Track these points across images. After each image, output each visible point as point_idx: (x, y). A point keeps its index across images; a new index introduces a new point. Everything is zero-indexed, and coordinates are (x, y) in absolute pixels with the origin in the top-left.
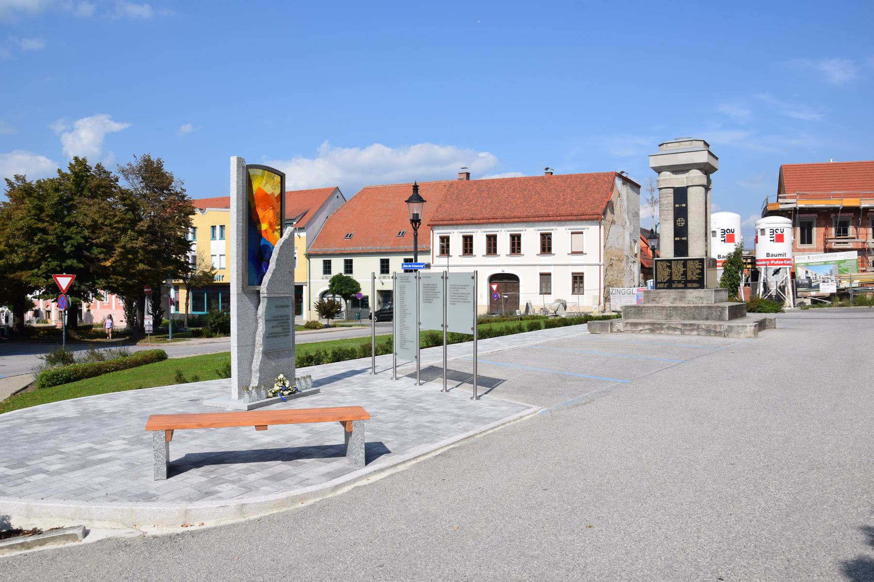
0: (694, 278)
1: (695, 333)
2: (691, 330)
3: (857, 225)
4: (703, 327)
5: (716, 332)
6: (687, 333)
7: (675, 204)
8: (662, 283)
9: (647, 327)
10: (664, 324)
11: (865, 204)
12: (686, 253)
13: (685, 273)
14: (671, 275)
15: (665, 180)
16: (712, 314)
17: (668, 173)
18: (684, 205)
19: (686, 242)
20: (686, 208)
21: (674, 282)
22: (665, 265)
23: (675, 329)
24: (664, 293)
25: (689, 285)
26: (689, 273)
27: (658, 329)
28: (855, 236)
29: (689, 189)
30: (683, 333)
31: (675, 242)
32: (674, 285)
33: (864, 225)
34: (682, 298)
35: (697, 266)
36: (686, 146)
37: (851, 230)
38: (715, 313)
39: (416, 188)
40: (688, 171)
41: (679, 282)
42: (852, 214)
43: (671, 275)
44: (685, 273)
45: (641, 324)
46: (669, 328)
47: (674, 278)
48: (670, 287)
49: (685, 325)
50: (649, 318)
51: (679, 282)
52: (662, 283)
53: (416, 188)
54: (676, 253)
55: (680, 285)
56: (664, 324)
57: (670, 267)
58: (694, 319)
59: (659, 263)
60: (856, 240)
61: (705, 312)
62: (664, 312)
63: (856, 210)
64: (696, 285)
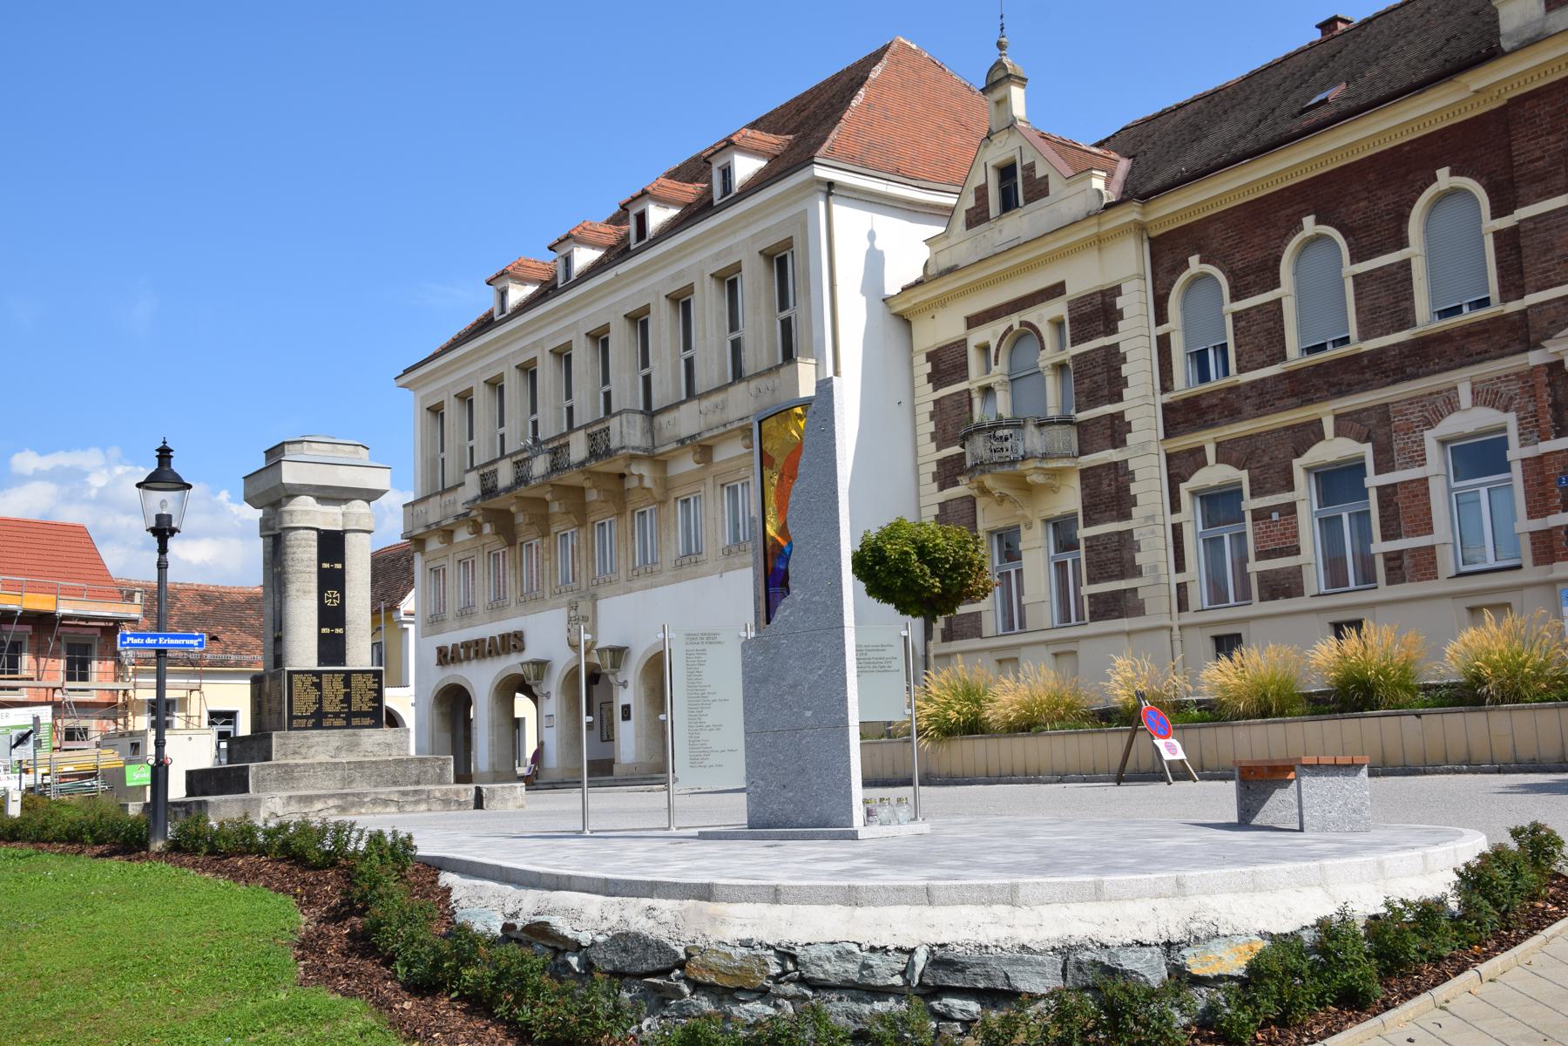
0: (365, 708)
1: (423, 807)
2: (417, 802)
3: (39, 652)
4: (438, 794)
5: (460, 804)
6: (408, 808)
7: (320, 562)
8: (302, 717)
9: (331, 803)
10: (366, 795)
11: (64, 609)
12: (341, 659)
13: (347, 699)
14: (320, 701)
15: (307, 512)
16: (426, 772)
17: (311, 500)
18: (338, 566)
19: (343, 637)
20: (342, 572)
21: (325, 715)
22: (308, 683)
23: (386, 803)
24: (316, 736)
25: (355, 721)
26: (356, 699)
27: (353, 805)
28: (33, 674)
29: (348, 537)
30: (400, 808)
31: (321, 636)
32: (326, 723)
33: (55, 655)
34: (352, 747)
35: (370, 684)
36: (344, 453)
37: (26, 660)
38: (431, 771)
39: (164, 454)
40: (346, 501)
41: (336, 715)
42: (29, 628)
43: (320, 701)
44: (347, 699)
45: (319, 797)
46: (375, 802)
47: (327, 708)
48: (318, 726)
49: (404, 793)
50: (306, 787)
51: (336, 715)
52: (302, 717)
53: (164, 454)
54: (323, 658)
55: (338, 722)
56: (366, 795)
57: (318, 686)
58: (395, 783)
59: (296, 677)
60: (35, 683)
61: (414, 770)
62: (338, 774)
63: (42, 622)
64: (368, 721)
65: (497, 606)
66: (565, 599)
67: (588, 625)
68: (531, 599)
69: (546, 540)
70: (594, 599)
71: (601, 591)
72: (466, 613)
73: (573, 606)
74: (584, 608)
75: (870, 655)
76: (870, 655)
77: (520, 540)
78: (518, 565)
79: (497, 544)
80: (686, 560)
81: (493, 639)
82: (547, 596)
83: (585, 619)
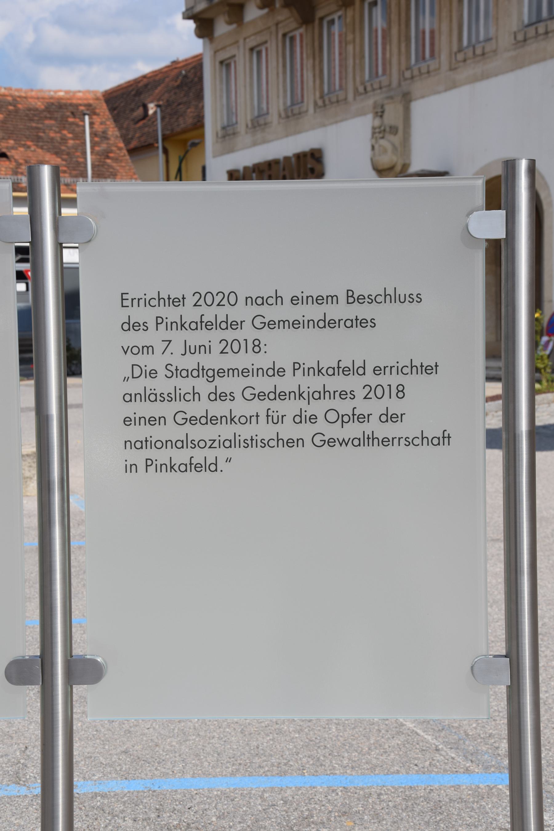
65: (293, 115)
66: (370, 102)
67: (397, 139)
68: (331, 103)
69: (350, 13)
70: (407, 99)
71: (417, 87)
72: (258, 124)
73: (380, 113)
74: (393, 114)
75: (282, 347)
76: (282, 347)
77: (319, 14)
78: (317, 52)
79: (286, 17)
80: (531, 31)
81: (287, 159)
82: (350, 96)
83: (394, 130)
